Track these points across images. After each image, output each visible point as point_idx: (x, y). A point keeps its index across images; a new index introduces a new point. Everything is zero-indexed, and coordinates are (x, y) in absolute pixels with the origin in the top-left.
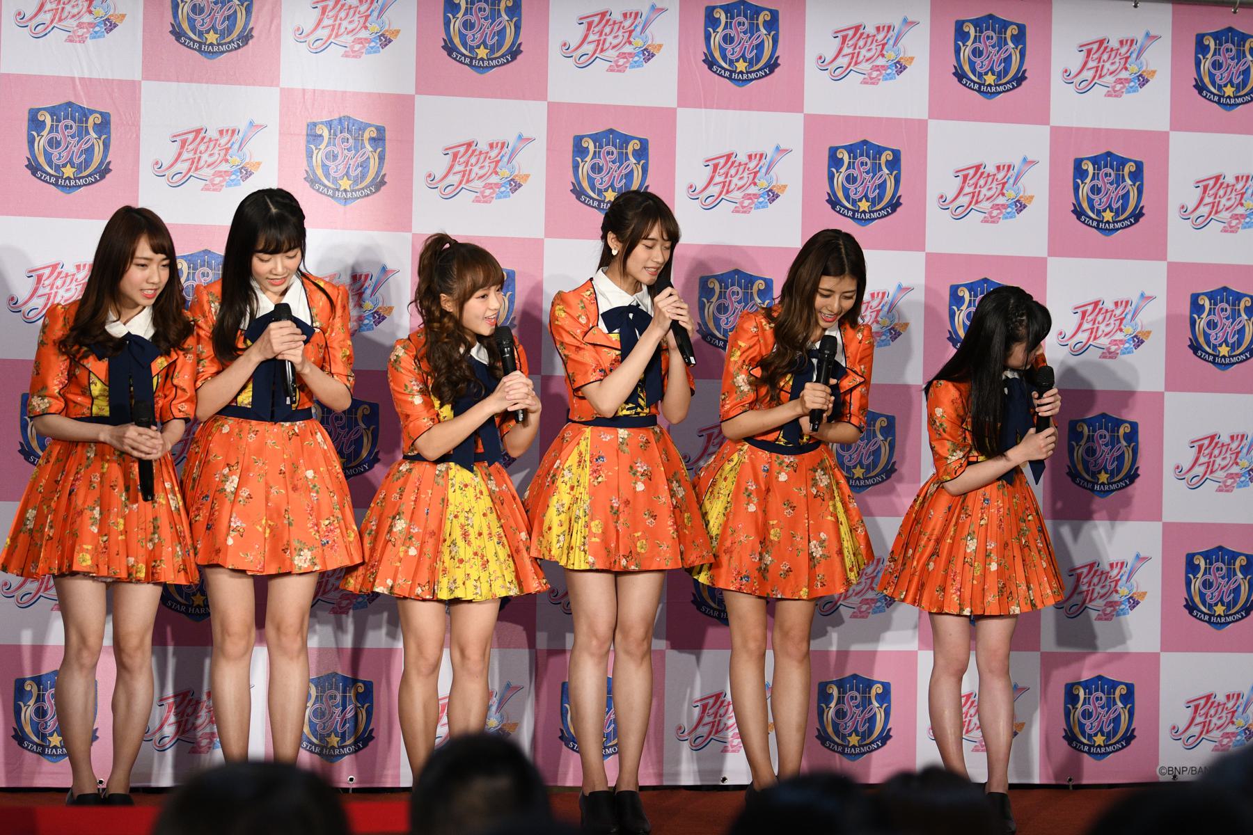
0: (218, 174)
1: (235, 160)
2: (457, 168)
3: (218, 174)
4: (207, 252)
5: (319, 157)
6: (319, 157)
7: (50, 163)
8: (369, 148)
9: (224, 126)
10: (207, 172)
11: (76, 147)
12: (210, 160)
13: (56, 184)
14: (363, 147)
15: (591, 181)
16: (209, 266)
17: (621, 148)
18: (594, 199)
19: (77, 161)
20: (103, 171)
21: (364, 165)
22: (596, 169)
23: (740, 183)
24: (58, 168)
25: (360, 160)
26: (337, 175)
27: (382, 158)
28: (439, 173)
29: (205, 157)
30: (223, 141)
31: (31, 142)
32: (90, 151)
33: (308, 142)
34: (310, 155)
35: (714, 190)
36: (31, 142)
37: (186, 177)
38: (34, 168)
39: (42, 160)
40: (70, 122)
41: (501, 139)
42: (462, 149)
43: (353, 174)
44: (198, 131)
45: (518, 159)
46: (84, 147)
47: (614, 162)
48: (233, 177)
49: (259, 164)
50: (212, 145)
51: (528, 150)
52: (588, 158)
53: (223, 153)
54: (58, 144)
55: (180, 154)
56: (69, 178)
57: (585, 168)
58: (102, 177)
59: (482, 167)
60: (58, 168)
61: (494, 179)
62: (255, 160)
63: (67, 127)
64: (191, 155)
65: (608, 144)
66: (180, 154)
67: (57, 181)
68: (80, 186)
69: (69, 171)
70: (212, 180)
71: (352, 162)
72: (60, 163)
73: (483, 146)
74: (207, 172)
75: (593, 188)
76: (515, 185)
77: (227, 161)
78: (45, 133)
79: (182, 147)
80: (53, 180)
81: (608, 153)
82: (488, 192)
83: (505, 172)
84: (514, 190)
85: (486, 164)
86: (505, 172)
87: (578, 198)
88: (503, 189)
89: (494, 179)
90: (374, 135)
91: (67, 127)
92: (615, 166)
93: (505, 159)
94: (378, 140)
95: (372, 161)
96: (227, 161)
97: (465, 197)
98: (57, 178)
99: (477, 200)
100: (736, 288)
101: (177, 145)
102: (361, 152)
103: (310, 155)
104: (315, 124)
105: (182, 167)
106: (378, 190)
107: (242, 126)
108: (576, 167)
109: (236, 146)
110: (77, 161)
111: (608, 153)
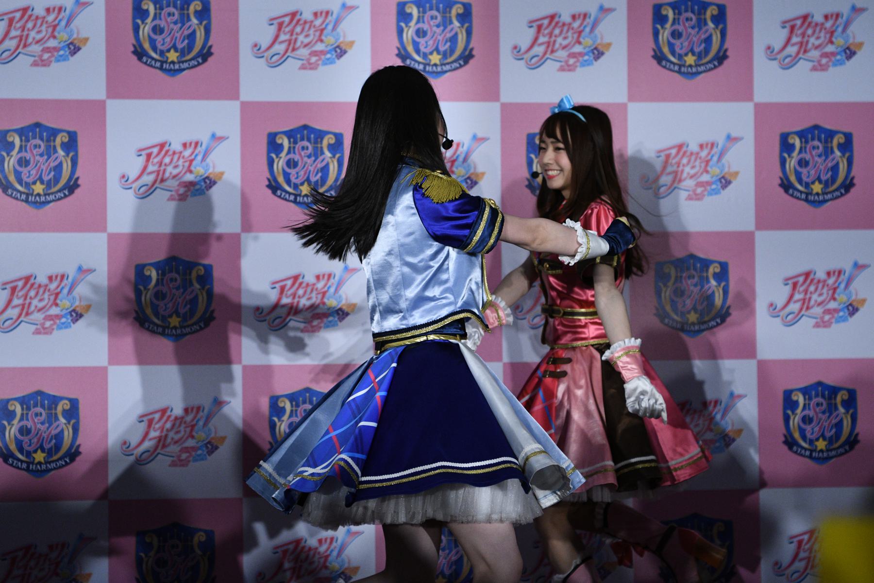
0: (314, 53)
1: (329, 39)
2: (542, 39)
3: (314, 53)
4: (305, 127)
5: (409, 33)
6: (409, 33)
7: (155, 49)
8: (456, 24)
9: (319, 8)
10: (304, 52)
11: (179, 33)
12: (307, 41)
13: (161, 68)
14: (451, 22)
15: (671, 46)
16: (309, 140)
17: (699, 14)
18: (674, 64)
19: (180, 46)
20: (205, 55)
21: (454, 39)
22: (676, 35)
23: (817, 43)
24: (162, 53)
25: (449, 35)
26: (427, 51)
27: (469, 33)
28: (524, 48)
29: (301, 38)
30: (318, 22)
31: (136, 29)
32: (192, 36)
33: (398, 21)
34: (400, 32)
35: (792, 50)
36: (136, 29)
37: (283, 58)
38: (139, 53)
39: (147, 46)
40: (172, 10)
41: (583, 10)
42: (546, 22)
43: (442, 49)
44: (293, 15)
45: (600, 28)
46: (186, 33)
47: (693, 28)
48: (329, 56)
49: (352, 43)
50: (307, 26)
51: (609, 19)
52: (668, 25)
53: (318, 34)
54: (161, 31)
55: (277, 37)
56: (173, 63)
57: (665, 35)
58: (205, 60)
59: (565, 38)
60: (162, 53)
61: (577, 49)
62: (349, 39)
63: (169, 14)
64: (287, 37)
65: (686, 11)
66: (277, 37)
67: (162, 66)
68: (184, 70)
69: (173, 56)
70: (308, 60)
71: (440, 38)
72: (164, 48)
73: (566, 18)
74: (304, 52)
75: (673, 53)
76: (598, 53)
77: (322, 41)
78: (149, 20)
79: (279, 29)
80: (158, 64)
81: (687, 19)
82: (571, 61)
83: (587, 41)
84: (597, 58)
85: (570, 34)
86: (587, 41)
87: (659, 63)
88: (586, 58)
89: (577, 49)
90: (461, 11)
91: (169, 14)
92: (693, 32)
93: (588, 30)
94: (466, 16)
95: (460, 37)
96: (322, 41)
97: (551, 66)
98: (162, 62)
99: (562, 69)
100: (816, 143)
101: (273, 30)
102: (449, 28)
103: (400, 32)
104: (405, 4)
105: (280, 48)
106: (466, 62)
107: (336, 8)
108: (656, 34)
109: (330, 27)
110: (180, 46)
111: (687, 19)
